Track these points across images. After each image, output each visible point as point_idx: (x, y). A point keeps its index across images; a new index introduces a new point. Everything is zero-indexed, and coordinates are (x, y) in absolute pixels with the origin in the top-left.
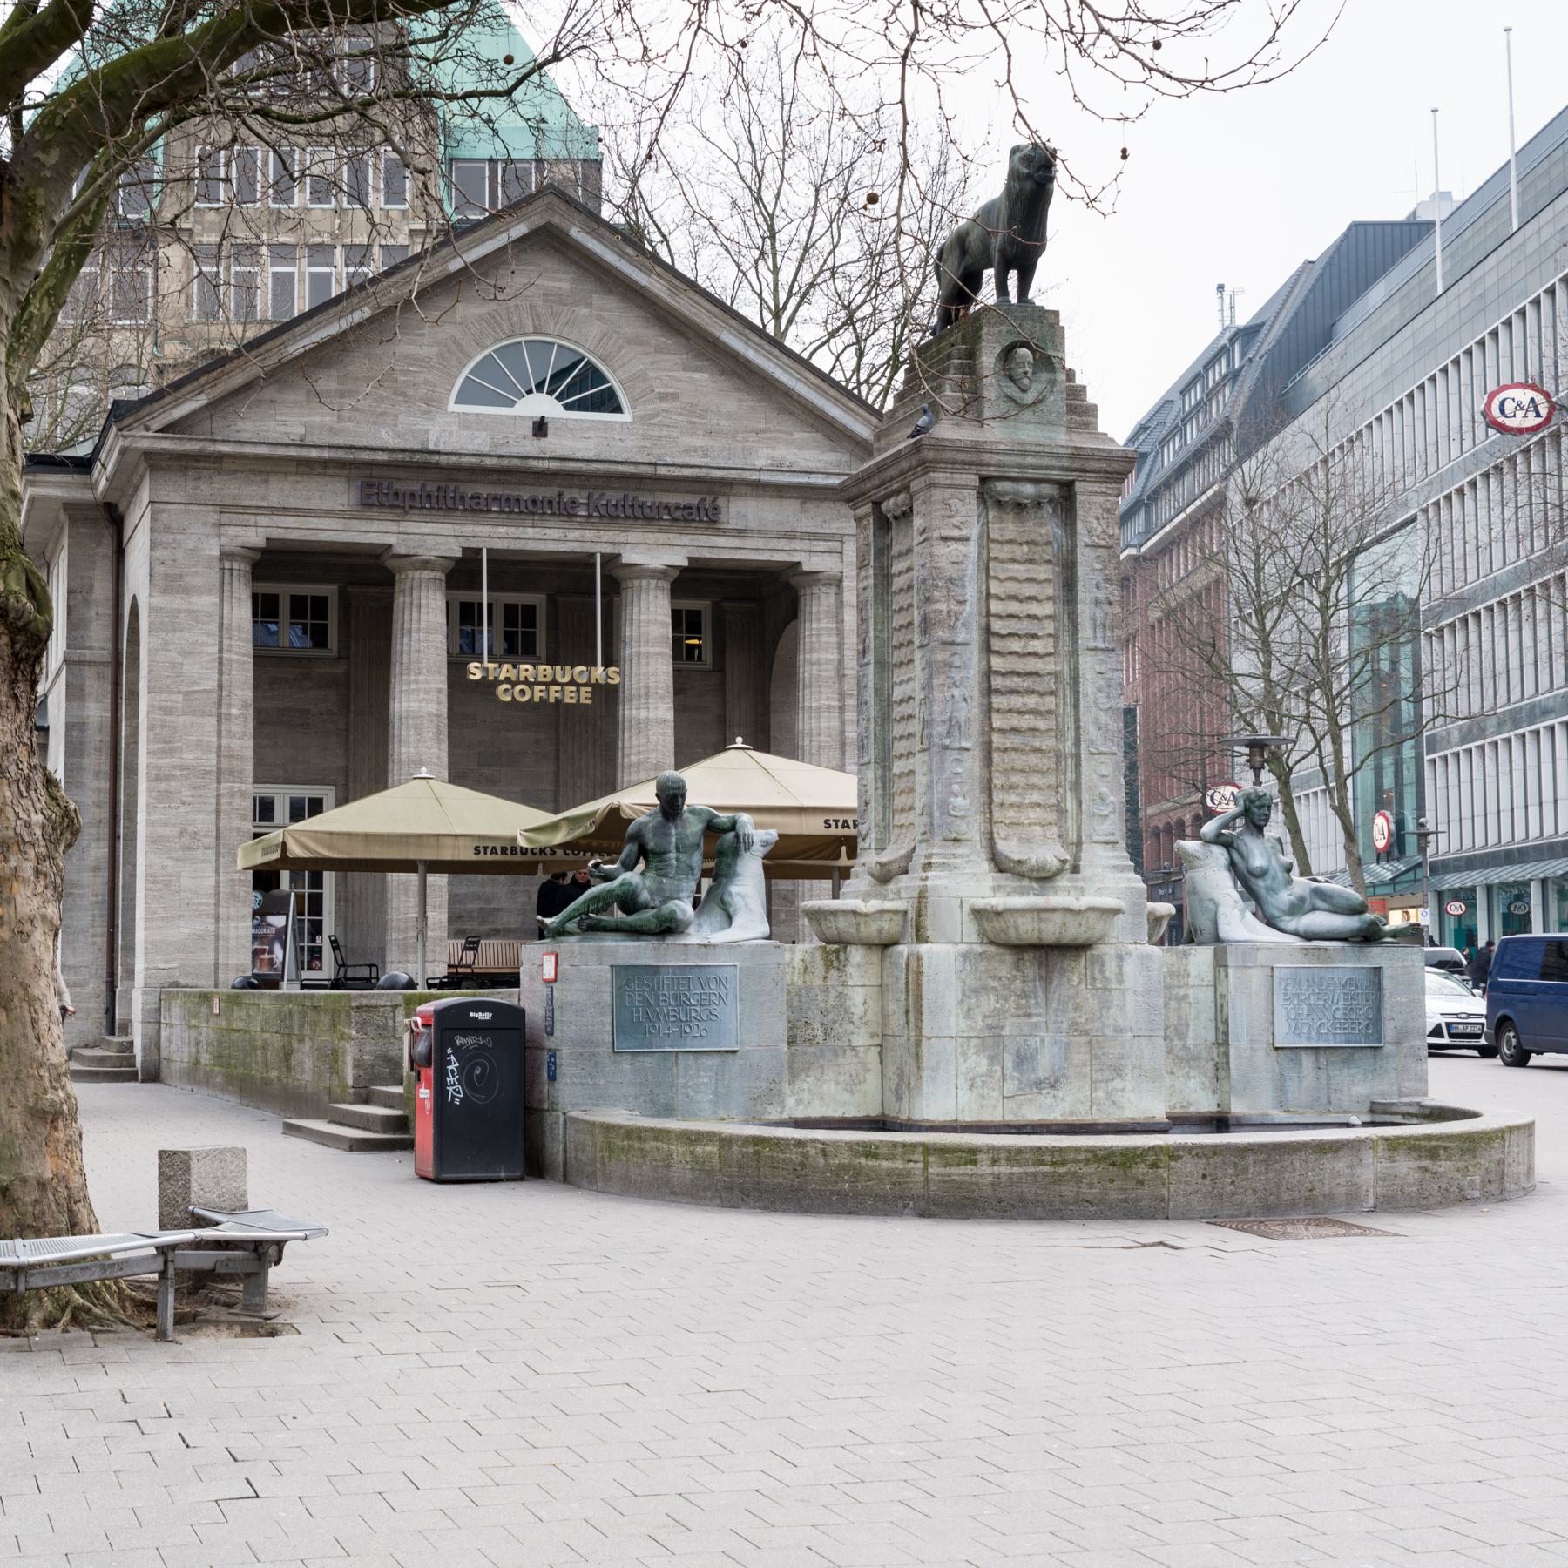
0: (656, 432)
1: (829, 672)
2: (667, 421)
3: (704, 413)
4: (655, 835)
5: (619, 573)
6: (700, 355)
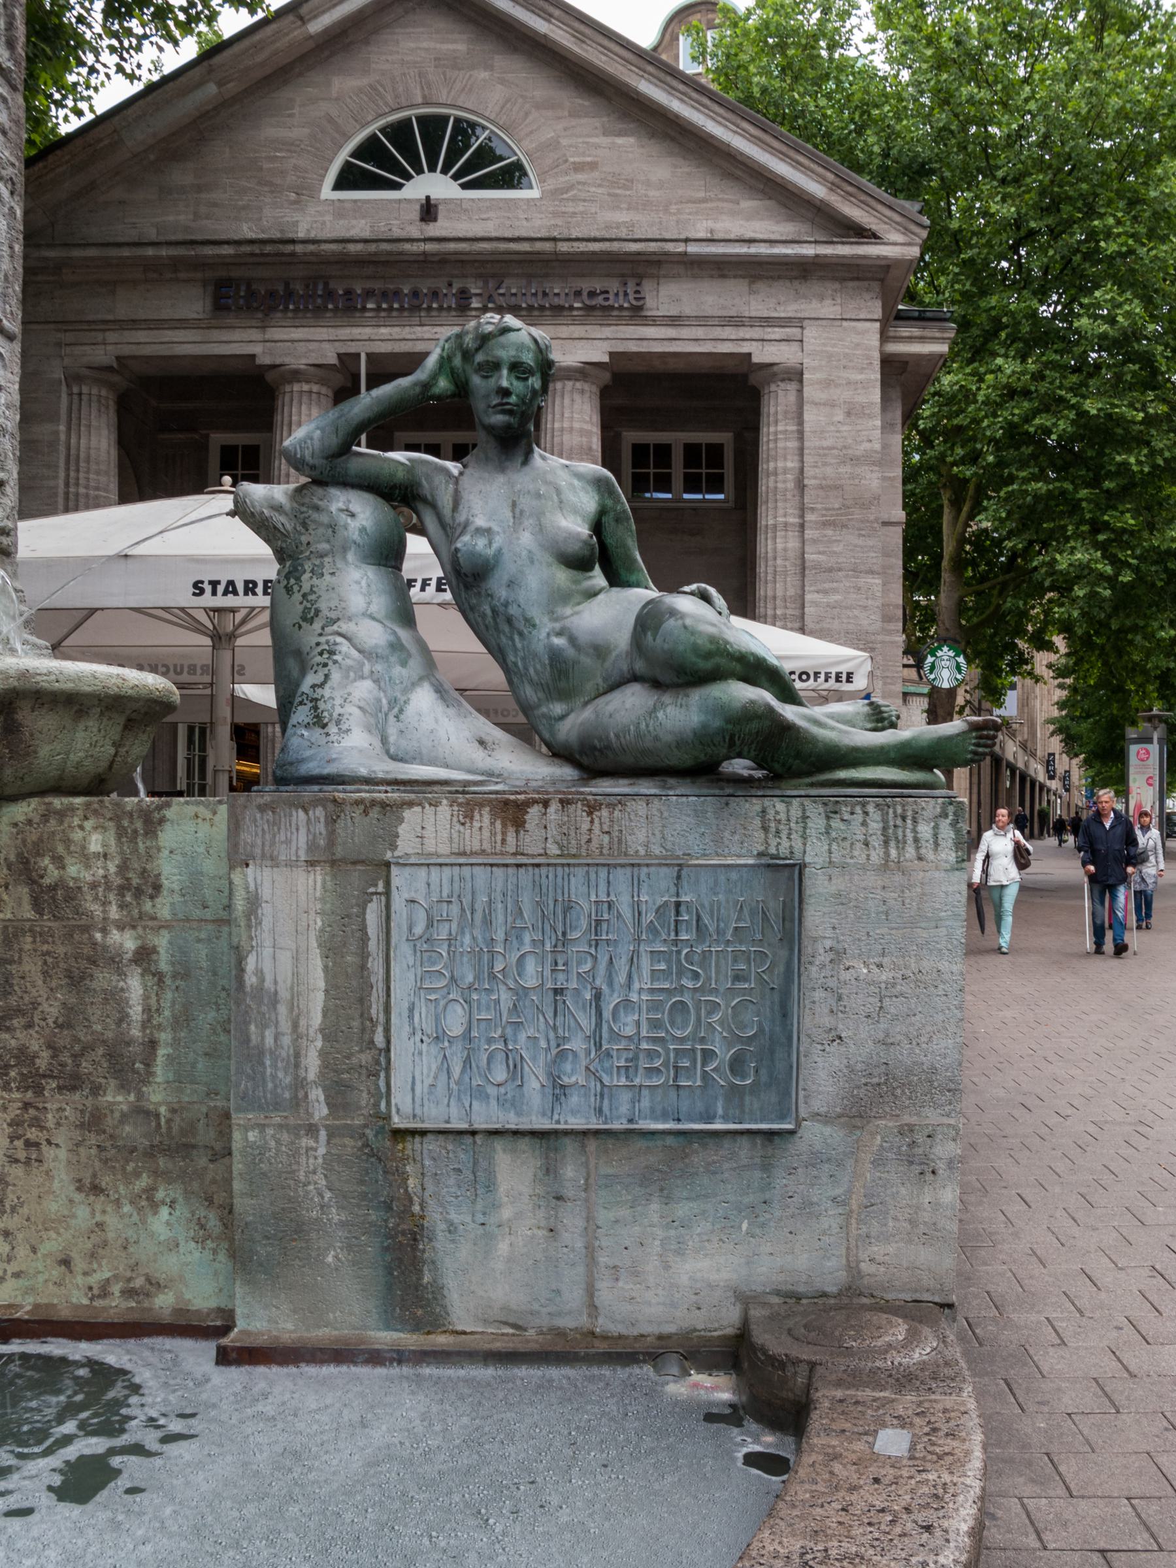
0: (570, 208)
1: (787, 483)
2: (583, 195)
3: (629, 183)
6: (625, 116)
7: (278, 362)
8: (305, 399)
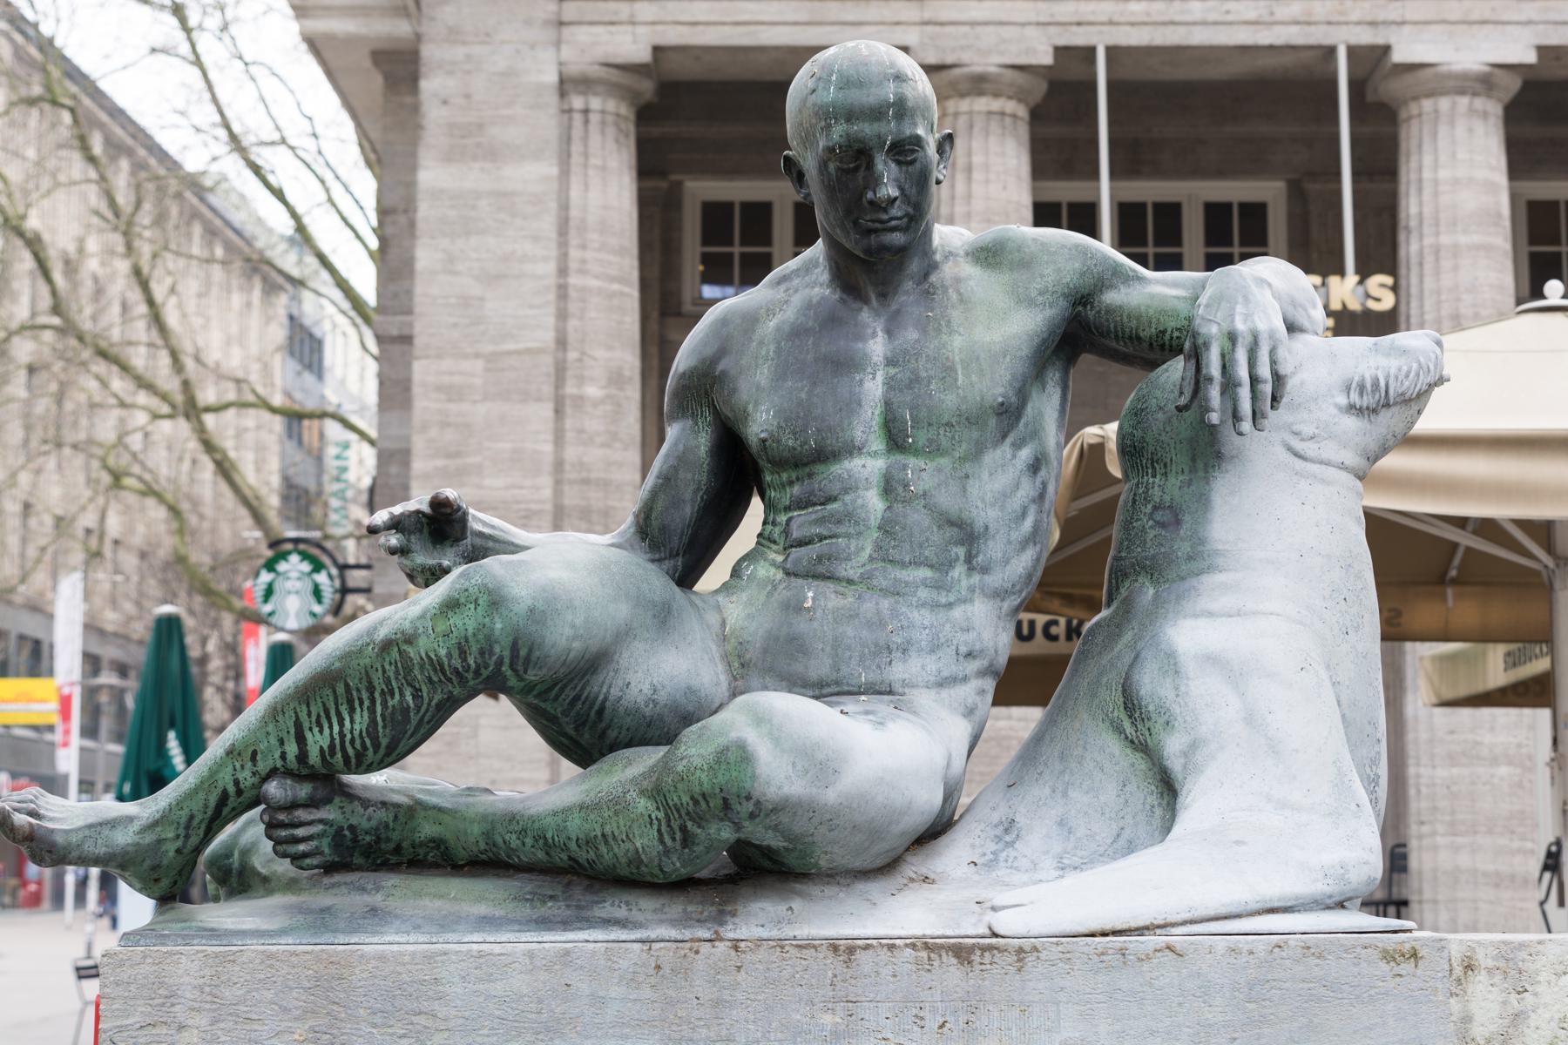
4: (780, 376)
5: (1392, 88)
7: (949, 60)
8: (994, 126)
